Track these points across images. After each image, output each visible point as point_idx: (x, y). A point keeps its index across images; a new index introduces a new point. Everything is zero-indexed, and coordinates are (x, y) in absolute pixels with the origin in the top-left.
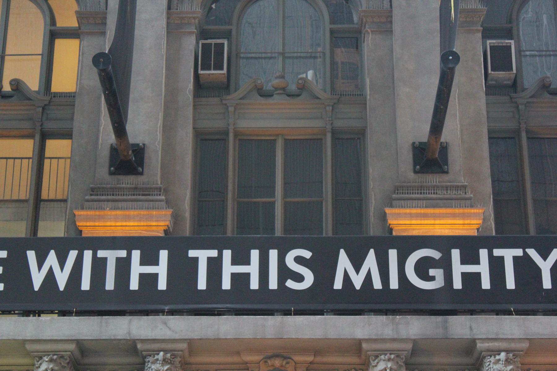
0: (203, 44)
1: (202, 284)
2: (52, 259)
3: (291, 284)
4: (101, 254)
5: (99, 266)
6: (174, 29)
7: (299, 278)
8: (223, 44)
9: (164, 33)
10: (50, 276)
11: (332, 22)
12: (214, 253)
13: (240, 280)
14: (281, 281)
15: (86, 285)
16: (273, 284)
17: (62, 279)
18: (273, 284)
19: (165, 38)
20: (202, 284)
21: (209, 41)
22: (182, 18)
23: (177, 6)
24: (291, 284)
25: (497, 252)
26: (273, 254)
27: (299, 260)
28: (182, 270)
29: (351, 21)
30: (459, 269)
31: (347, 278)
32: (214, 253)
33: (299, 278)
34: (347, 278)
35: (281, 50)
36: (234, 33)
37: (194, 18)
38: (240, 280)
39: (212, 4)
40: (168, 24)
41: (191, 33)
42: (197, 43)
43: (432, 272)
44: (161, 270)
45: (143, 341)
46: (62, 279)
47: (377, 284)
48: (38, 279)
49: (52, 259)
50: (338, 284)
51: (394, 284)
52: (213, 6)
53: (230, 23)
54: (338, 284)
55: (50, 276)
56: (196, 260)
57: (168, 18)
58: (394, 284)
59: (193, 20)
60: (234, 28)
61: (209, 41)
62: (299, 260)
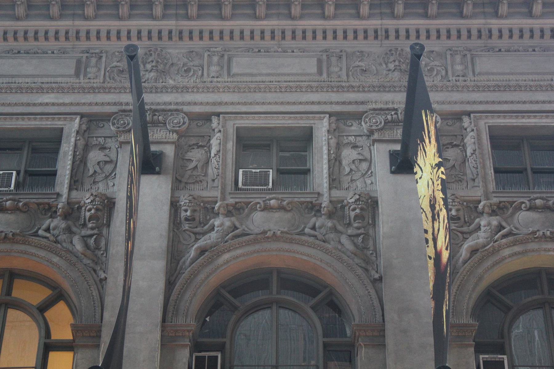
0: (196, 357)
6: (168, 342)
8: (217, 357)
9: (158, 345)
11: (325, 336)
19: (159, 351)
21: (202, 354)
22: (176, 331)
23: (172, 319)
29: (345, 336)
35: (274, 363)
36: (228, 346)
37: (189, 331)
39: (206, 317)
40: (162, 336)
41: (184, 346)
42: (191, 356)
52: (208, 319)
53: (224, 336)
57: (162, 331)
59: (187, 333)
60: (227, 340)
61: (202, 354)
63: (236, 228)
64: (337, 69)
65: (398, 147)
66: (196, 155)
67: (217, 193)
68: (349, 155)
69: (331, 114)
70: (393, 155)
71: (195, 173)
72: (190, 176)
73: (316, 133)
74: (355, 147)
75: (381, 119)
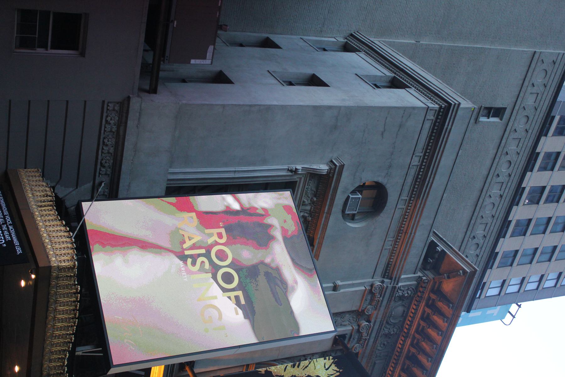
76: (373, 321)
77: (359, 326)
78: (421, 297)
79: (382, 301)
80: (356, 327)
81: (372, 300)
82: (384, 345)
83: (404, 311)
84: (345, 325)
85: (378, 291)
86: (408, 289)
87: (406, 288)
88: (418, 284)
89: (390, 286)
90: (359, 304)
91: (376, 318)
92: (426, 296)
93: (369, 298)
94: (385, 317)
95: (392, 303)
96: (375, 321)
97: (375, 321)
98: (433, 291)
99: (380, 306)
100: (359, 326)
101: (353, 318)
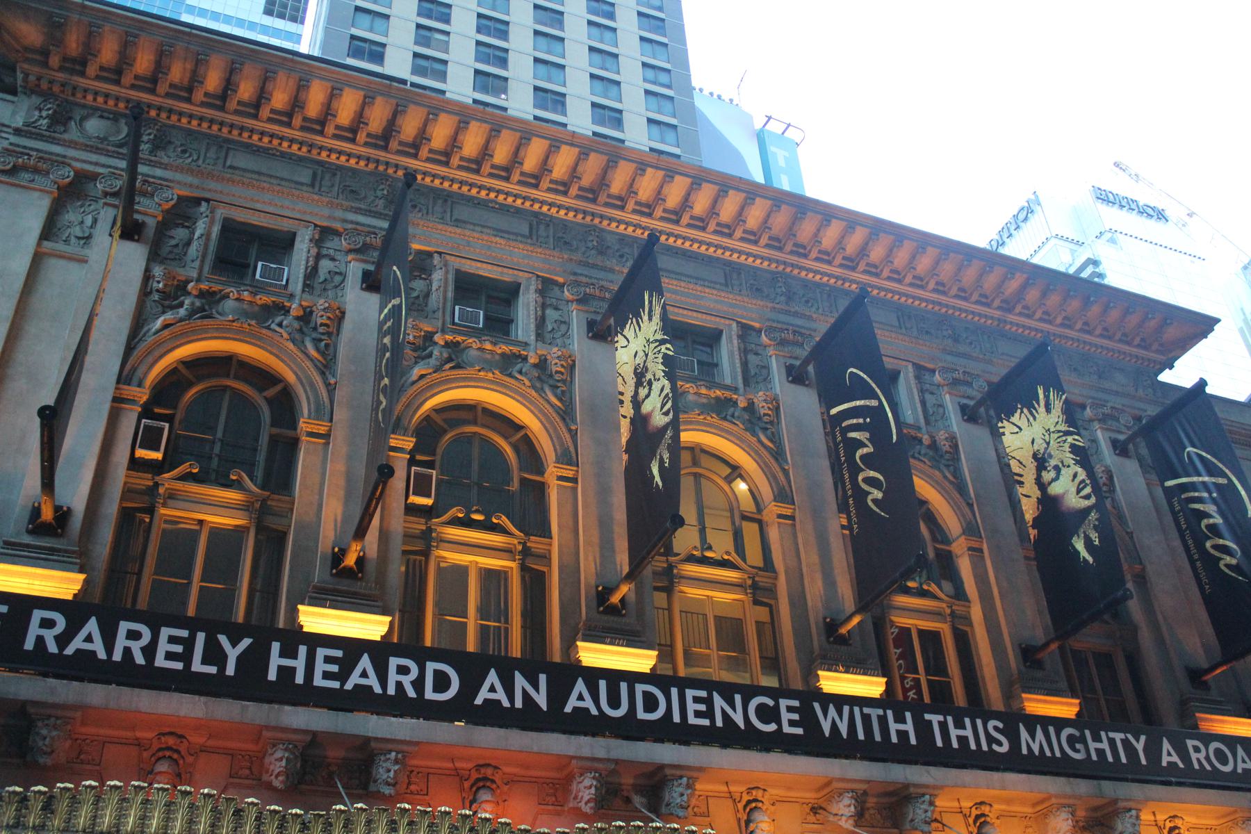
1: (939, 743)
2: (832, 711)
3: (995, 747)
4: (866, 710)
5: (866, 719)
7: (1000, 744)
10: (834, 726)
12: (941, 718)
13: (963, 740)
14: (989, 745)
15: (861, 736)
16: (985, 748)
17: (843, 728)
18: (985, 748)
20: (939, 743)
24: (995, 747)
25: (1111, 735)
26: (979, 722)
27: (996, 728)
28: (923, 729)
30: (1093, 746)
31: (1028, 745)
32: (941, 718)
33: (1000, 744)
34: (1028, 745)
38: (963, 740)
43: (1078, 746)
44: (909, 726)
45: (916, 786)
46: (843, 728)
47: (1048, 754)
48: (826, 728)
49: (832, 711)
50: (1025, 751)
51: (1058, 754)
54: (1025, 751)
55: (834, 726)
56: (930, 722)
58: (1058, 754)
62: (996, 728)
63: (205, 310)
64: (329, 184)
65: (372, 268)
66: (180, 234)
67: (195, 275)
68: (325, 265)
69: (316, 225)
70: (366, 275)
71: (176, 250)
72: (171, 252)
73: (298, 239)
74: (333, 259)
75: (361, 240)
76: (101, 170)
77: (106, 194)
78: (63, 85)
79: (37, 150)
80: (109, 200)
81: (36, 171)
82: (184, 152)
83: (101, 117)
84: (95, 221)
85: (12, 160)
86: (40, 110)
87: (37, 113)
88: (33, 92)
89: (13, 139)
90: (37, 194)
91: (96, 164)
92: (60, 75)
93: (27, 176)
94: (97, 148)
95: (66, 136)
96: (103, 166)
97: (103, 166)
98: (45, 64)
99: (64, 157)
100: (106, 194)
101: (81, 206)
